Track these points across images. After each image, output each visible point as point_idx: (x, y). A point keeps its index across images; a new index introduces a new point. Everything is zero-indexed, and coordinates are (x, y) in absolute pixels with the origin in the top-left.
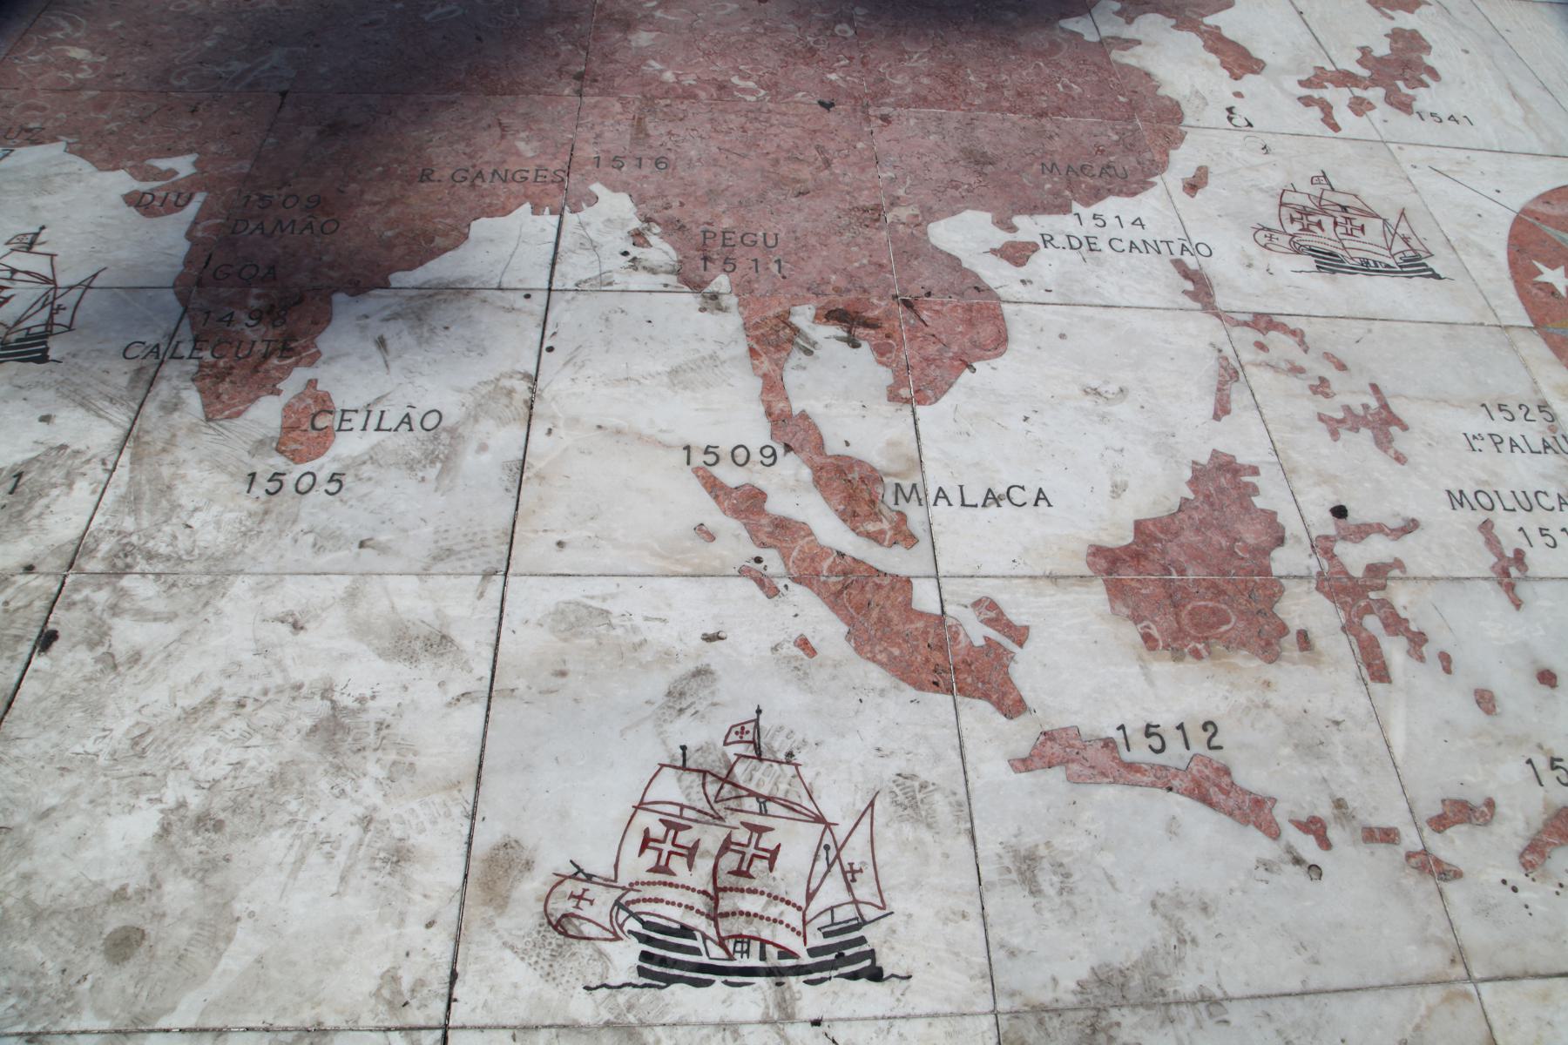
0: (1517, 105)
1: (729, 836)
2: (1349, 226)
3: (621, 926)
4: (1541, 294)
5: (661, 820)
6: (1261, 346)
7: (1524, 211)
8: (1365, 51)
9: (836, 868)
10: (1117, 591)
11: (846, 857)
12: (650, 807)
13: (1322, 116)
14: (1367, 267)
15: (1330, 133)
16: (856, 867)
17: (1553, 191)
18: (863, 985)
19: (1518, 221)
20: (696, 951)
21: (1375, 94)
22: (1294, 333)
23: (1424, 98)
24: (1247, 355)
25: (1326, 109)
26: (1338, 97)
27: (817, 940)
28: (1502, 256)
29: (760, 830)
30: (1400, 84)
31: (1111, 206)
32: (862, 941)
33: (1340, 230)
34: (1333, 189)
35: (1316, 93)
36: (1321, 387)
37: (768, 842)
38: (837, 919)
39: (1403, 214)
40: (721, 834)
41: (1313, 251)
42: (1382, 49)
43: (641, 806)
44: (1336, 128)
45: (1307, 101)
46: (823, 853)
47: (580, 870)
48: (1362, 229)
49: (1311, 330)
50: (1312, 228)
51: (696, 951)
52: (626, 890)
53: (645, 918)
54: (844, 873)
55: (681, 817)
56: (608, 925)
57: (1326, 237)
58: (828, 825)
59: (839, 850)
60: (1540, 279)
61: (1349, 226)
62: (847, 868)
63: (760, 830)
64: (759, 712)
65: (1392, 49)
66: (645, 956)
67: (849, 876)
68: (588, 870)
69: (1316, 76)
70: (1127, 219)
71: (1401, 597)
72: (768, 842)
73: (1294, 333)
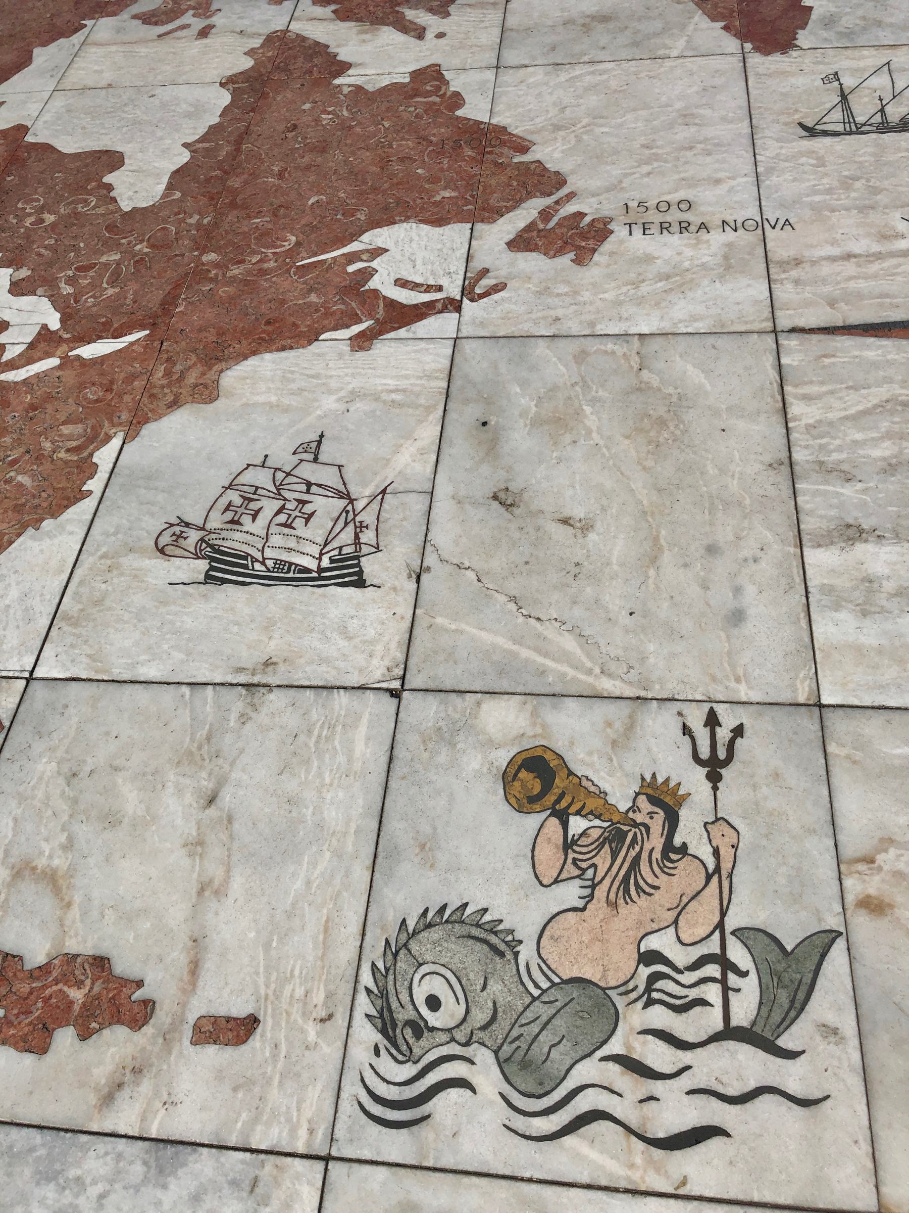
1: (284, 505)
3: (201, 550)
5: (241, 496)
9: (351, 527)
11: (358, 519)
12: (236, 487)
16: (364, 524)
18: (351, 590)
20: (245, 567)
27: (325, 563)
29: (304, 502)
32: (358, 565)
37: (308, 509)
38: (344, 552)
40: (278, 504)
43: (230, 487)
46: (344, 514)
47: (182, 521)
51: (245, 567)
52: (210, 532)
53: (217, 547)
54: (356, 527)
55: (255, 493)
56: (194, 551)
58: (352, 501)
59: (355, 515)
62: (358, 524)
63: (304, 502)
64: (322, 436)
66: (212, 568)
67: (358, 530)
68: (187, 519)
72: (308, 509)
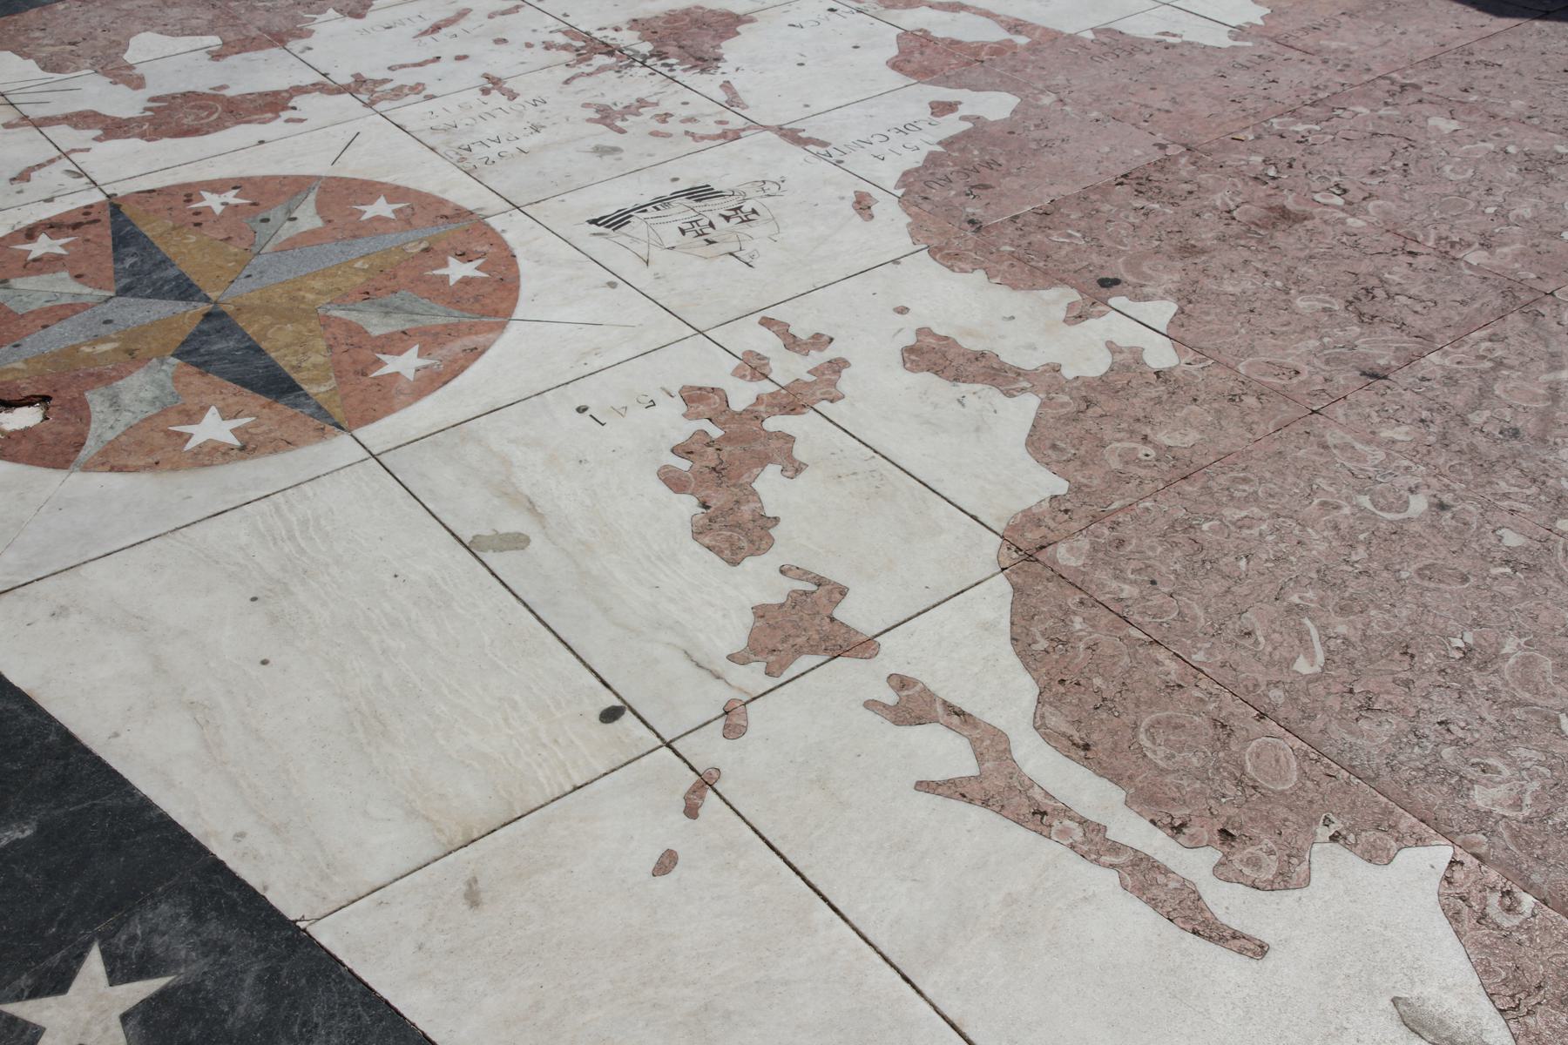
0: (525, 489)
2: (697, 228)
4: (479, 249)
6: (721, 122)
7: (502, 327)
8: (795, 469)
10: (730, 15)
13: (792, 330)
14: (661, 202)
15: (769, 313)
17: (463, 369)
19: (508, 315)
21: (742, 395)
22: (703, 138)
23: (675, 424)
24: (728, 116)
25: (792, 343)
26: (789, 368)
28: (524, 265)
30: (716, 432)
31: (914, 160)
33: (705, 222)
34: (731, 254)
35: (817, 358)
36: (665, 118)
39: (647, 263)
41: (719, 194)
42: (770, 485)
44: (767, 322)
45: (820, 341)
48: (683, 232)
49: (691, 145)
50: (733, 213)
57: (713, 210)
60: (479, 262)
61: (697, 228)
65: (754, 493)
69: (833, 384)
70: (890, 157)
71: (568, 56)
73: (703, 138)
